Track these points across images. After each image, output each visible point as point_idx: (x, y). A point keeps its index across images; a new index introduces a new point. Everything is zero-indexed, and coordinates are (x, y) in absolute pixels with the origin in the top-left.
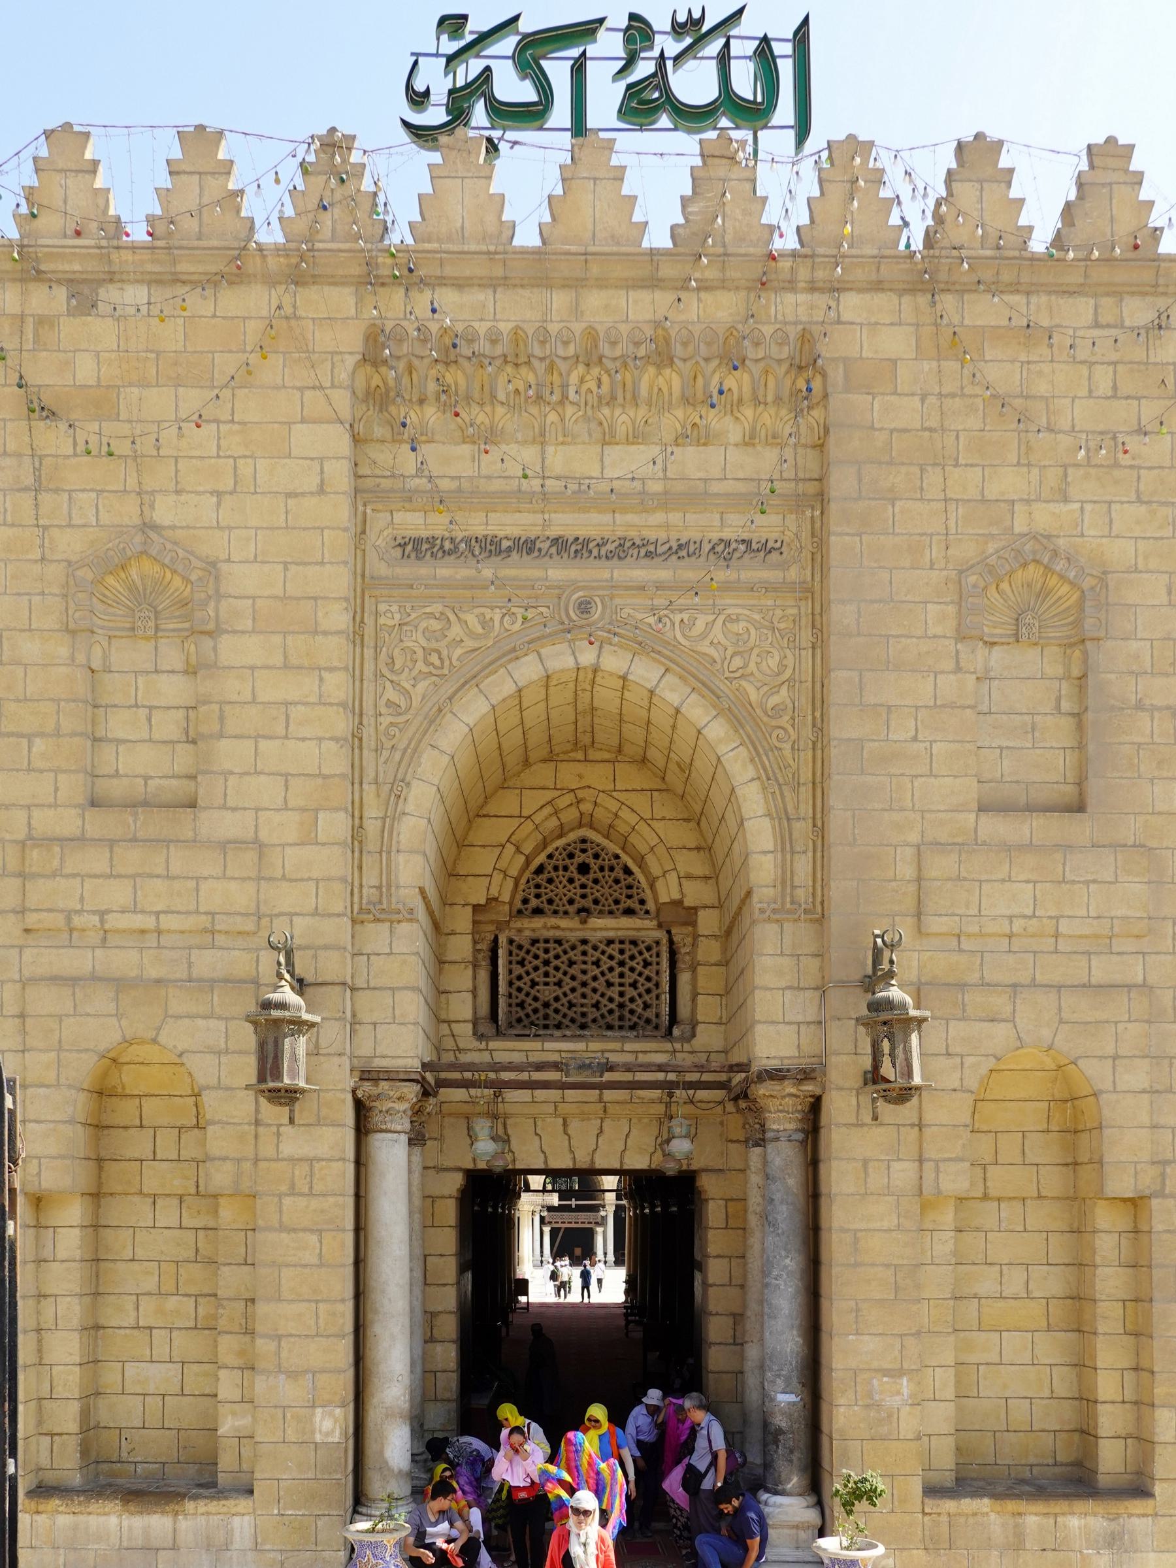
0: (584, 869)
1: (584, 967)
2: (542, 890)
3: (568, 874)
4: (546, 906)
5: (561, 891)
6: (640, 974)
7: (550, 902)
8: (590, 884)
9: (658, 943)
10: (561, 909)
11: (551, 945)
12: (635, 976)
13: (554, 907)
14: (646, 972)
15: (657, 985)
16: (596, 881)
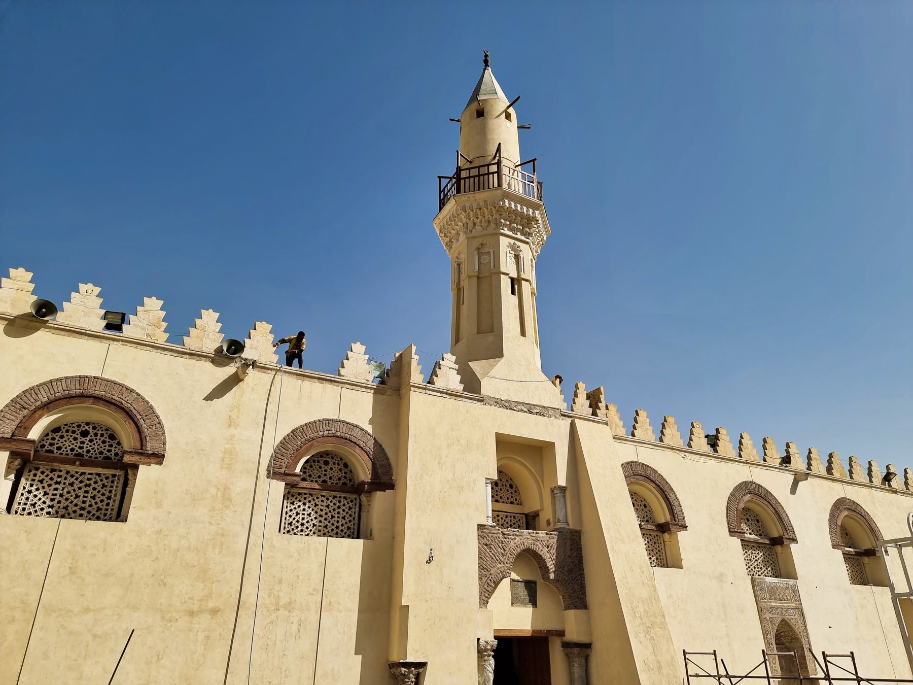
0: (326, 463)
1: (322, 508)
2: (307, 470)
3: (319, 465)
4: (308, 478)
5: (315, 471)
6: (347, 513)
7: (310, 476)
8: (329, 470)
9: (356, 499)
10: (314, 480)
11: (307, 496)
12: (344, 514)
13: (311, 479)
14: (350, 512)
15: (354, 519)
16: (331, 469)
